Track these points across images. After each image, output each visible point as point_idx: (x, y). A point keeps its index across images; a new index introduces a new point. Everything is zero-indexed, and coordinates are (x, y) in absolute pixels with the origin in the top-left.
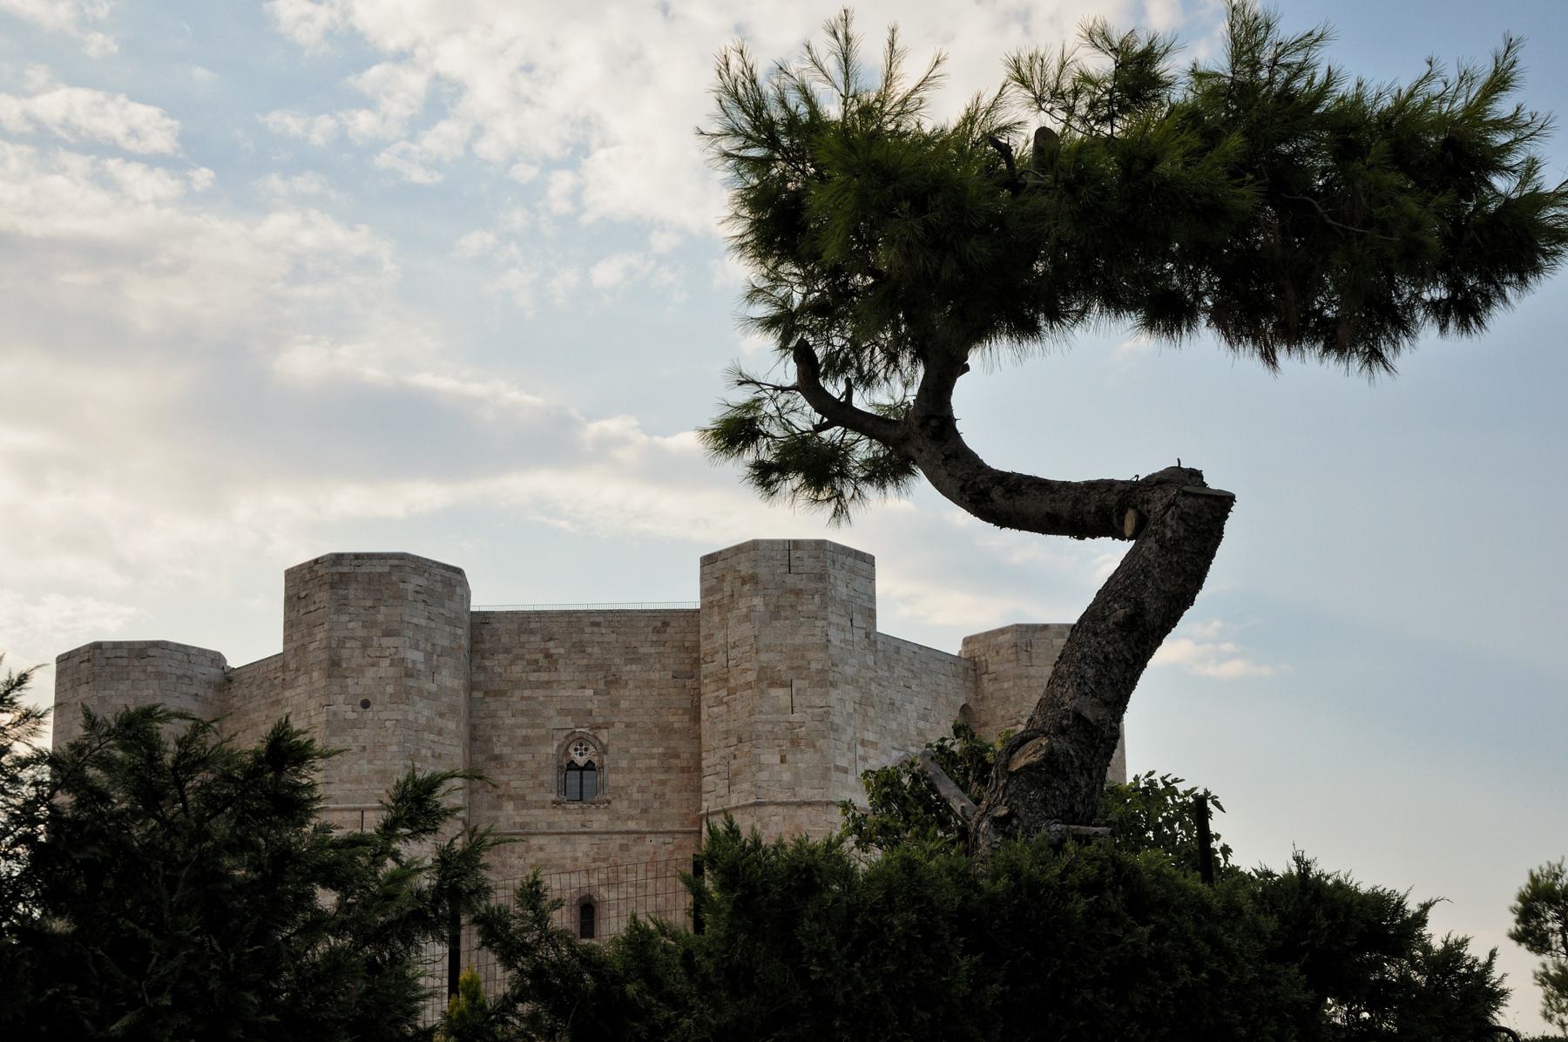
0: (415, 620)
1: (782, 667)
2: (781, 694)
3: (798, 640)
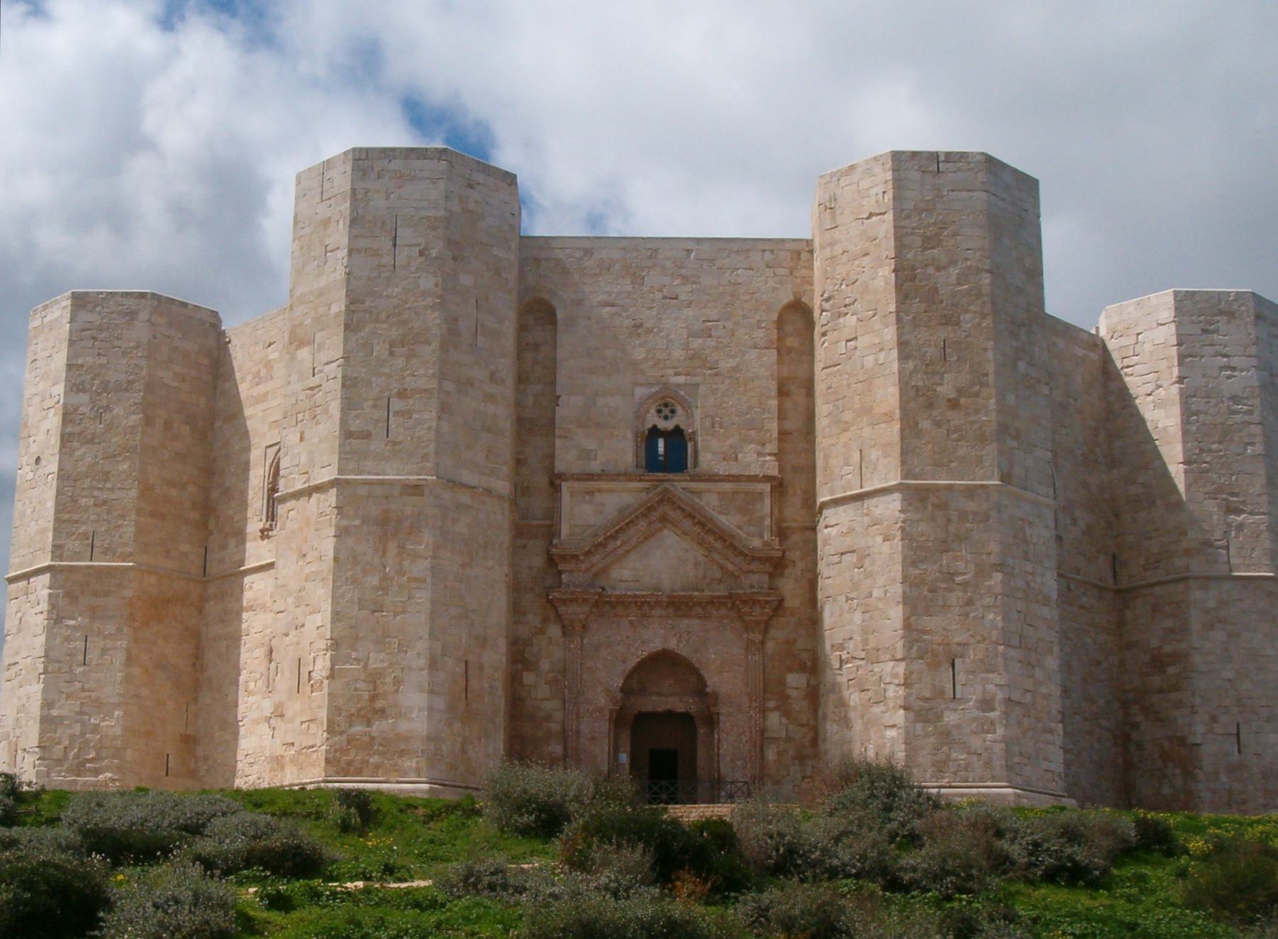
0: (80, 362)
2: (304, 353)
3: (323, 282)
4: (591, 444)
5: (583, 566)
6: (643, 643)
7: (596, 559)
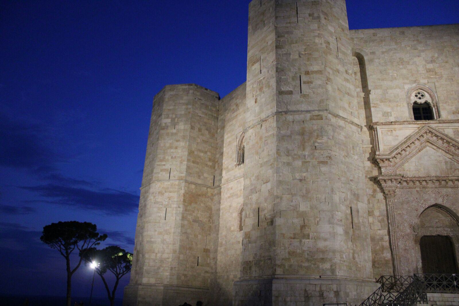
1: (257, 53)
4: (389, 110)
5: (392, 164)
6: (425, 201)
7: (396, 161)
